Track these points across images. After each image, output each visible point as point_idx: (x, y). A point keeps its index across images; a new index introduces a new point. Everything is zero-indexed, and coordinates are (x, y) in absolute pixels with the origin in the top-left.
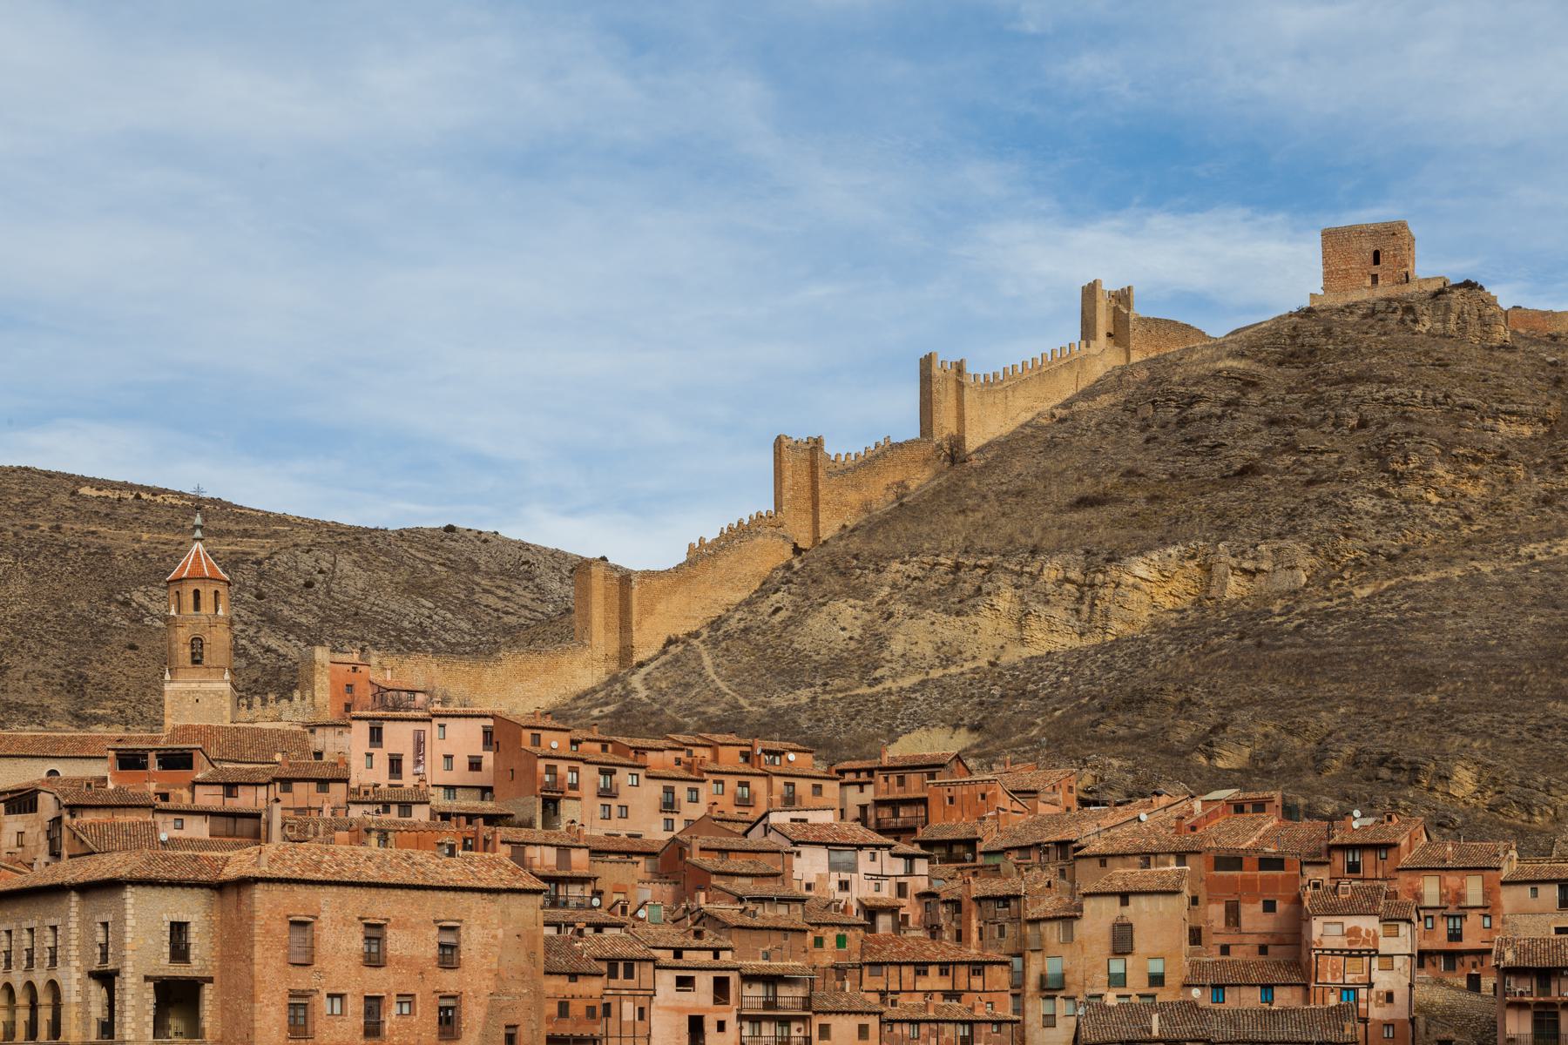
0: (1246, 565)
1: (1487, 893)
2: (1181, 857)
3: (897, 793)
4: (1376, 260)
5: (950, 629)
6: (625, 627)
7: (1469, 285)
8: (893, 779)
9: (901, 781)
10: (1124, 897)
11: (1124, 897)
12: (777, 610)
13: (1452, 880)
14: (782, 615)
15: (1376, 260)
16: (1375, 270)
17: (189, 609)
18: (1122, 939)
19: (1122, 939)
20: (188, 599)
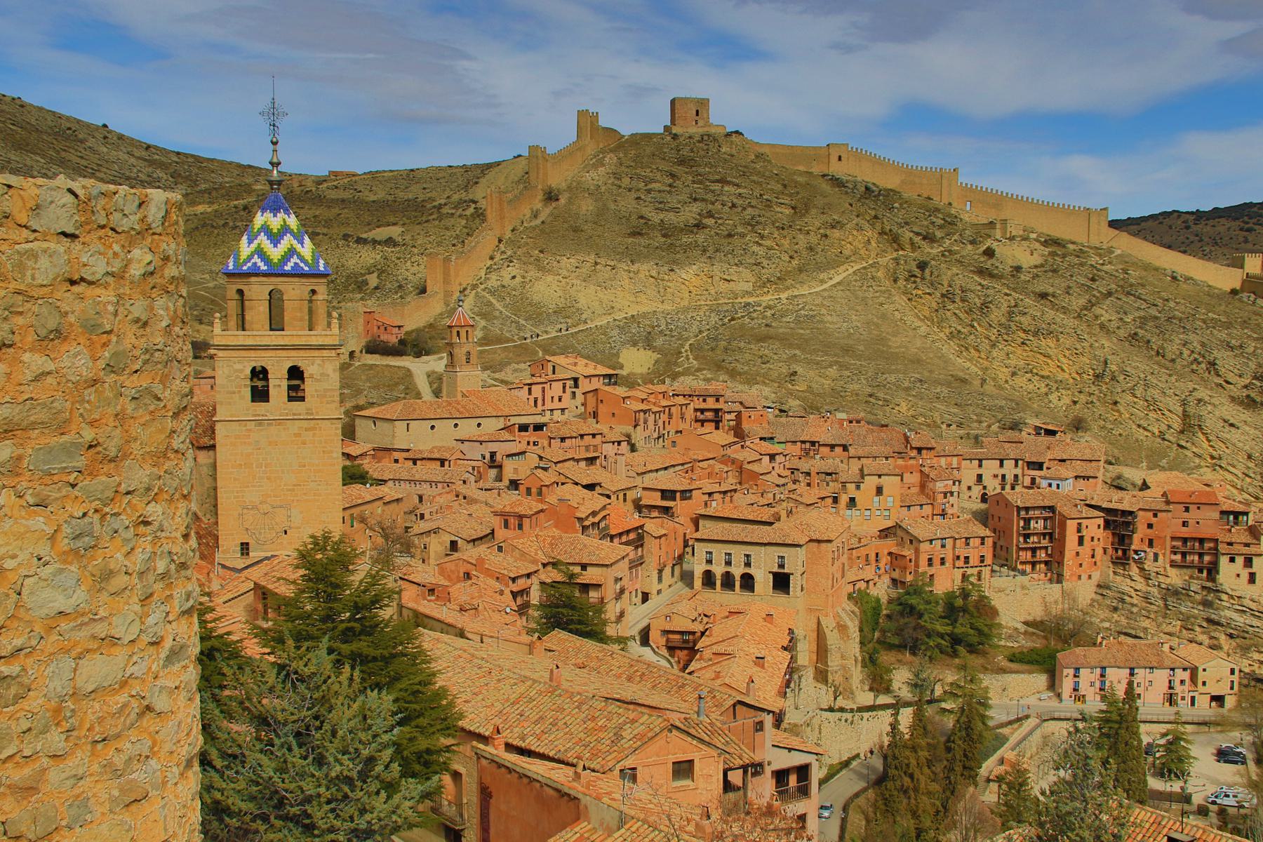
0: (726, 277)
1: (959, 464)
2: (887, 458)
3: (703, 406)
4: (697, 114)
5: (605, 296)
6: (446, 281)
7: (737, 132)
8: (701, 399)
9: (704, 401)
10: (880, 476)
11: (880, 476)
12: (514, 277)
13: (949, 458)
14: (518, 279)
15: (697, 114)
16: (697, 118)
17: (464, 339)
18: (879, 491)
19: (879, 491)
20: (455, 334)
